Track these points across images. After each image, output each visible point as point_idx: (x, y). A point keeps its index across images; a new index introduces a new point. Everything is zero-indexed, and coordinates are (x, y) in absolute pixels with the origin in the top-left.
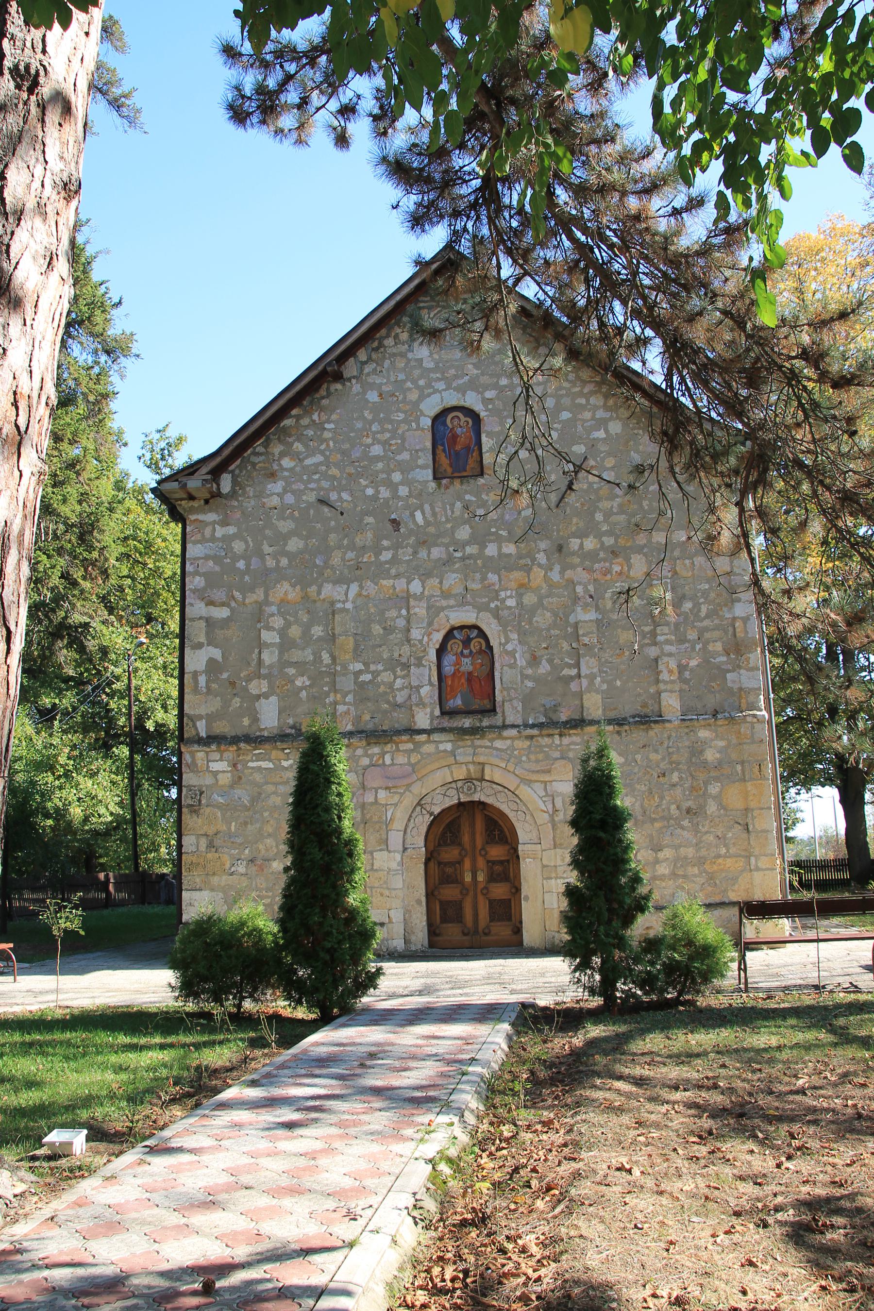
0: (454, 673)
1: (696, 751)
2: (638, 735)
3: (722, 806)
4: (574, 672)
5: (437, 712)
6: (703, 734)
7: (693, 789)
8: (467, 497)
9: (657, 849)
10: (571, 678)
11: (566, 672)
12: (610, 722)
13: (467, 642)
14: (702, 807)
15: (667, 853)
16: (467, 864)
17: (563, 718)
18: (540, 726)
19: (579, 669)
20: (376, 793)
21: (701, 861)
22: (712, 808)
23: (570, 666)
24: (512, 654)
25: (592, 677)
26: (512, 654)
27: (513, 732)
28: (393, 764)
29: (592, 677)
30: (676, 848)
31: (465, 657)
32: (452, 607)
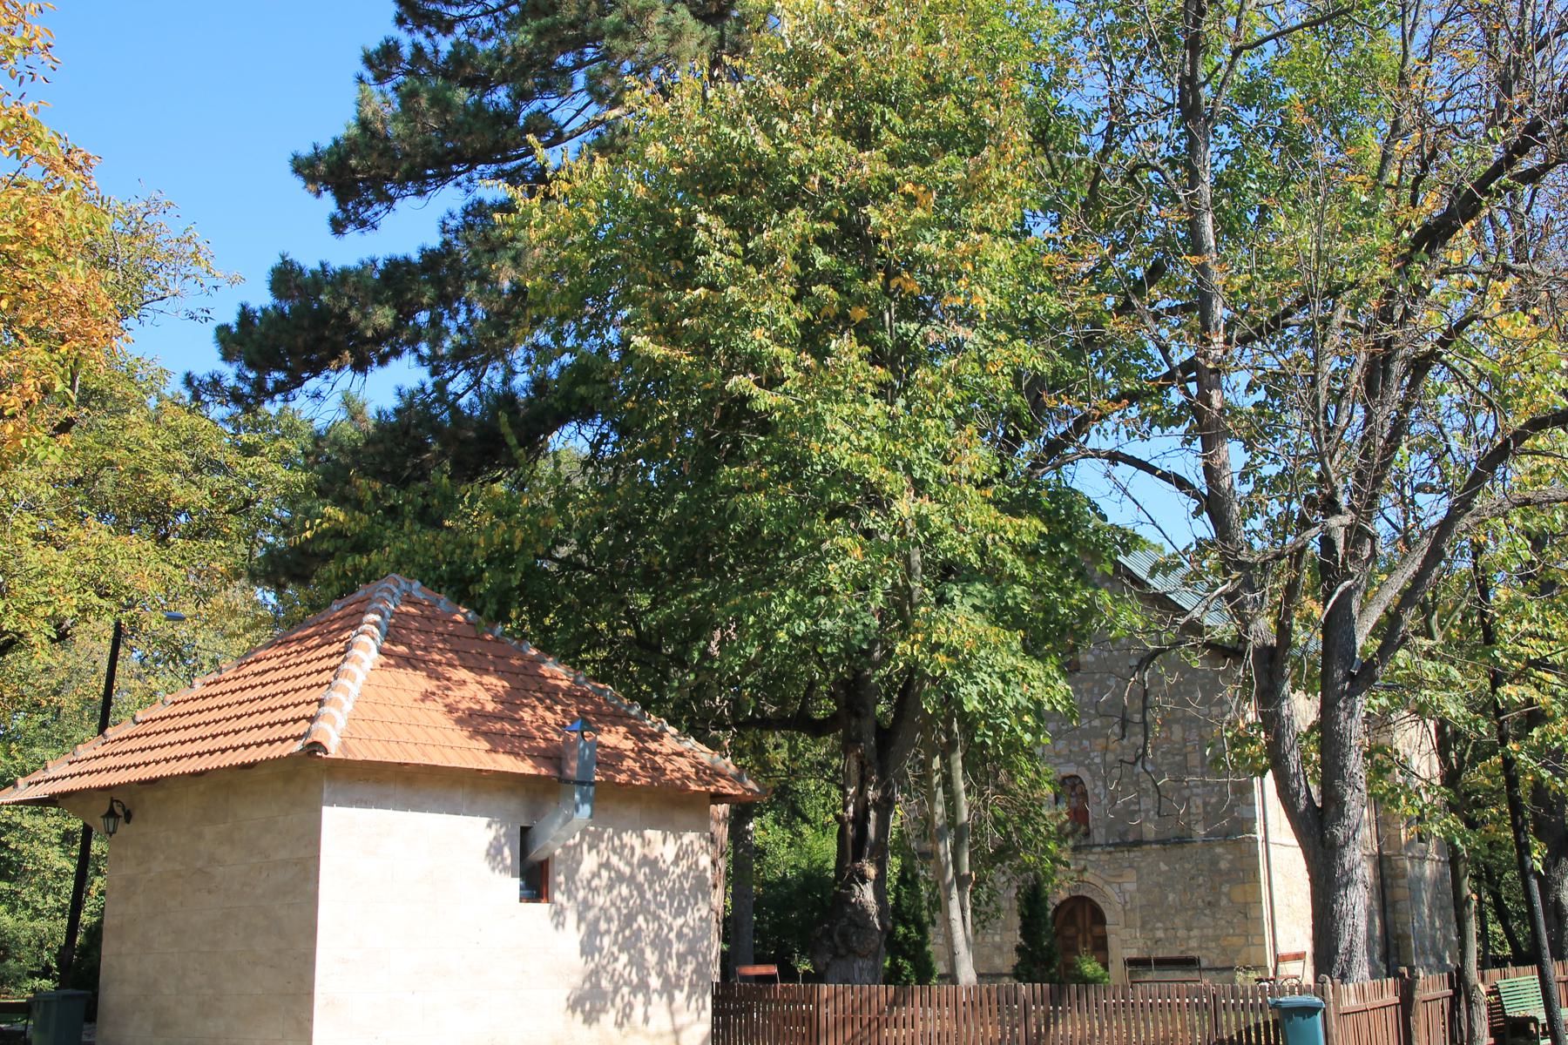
1: (1214, 862)
2: (1177, 852)
3: (1230, 900)
6: (1219, 850)
7: (1213, 888)
9: (1189, 929)
12: (1157, 842)
13: (1073, 787)
14: (1218, 901)
15: (1195, 932)
16: (1080, 938)
17: (1131, 838)
18: (1115, 845)
21: (1217, 938)
22: (1224, 902)
24: (1098, 796)
25: (1147, 811)
26: (1098, 796)
27: (1098, 849)
29: (1147, 811)
30: (1202, 928)
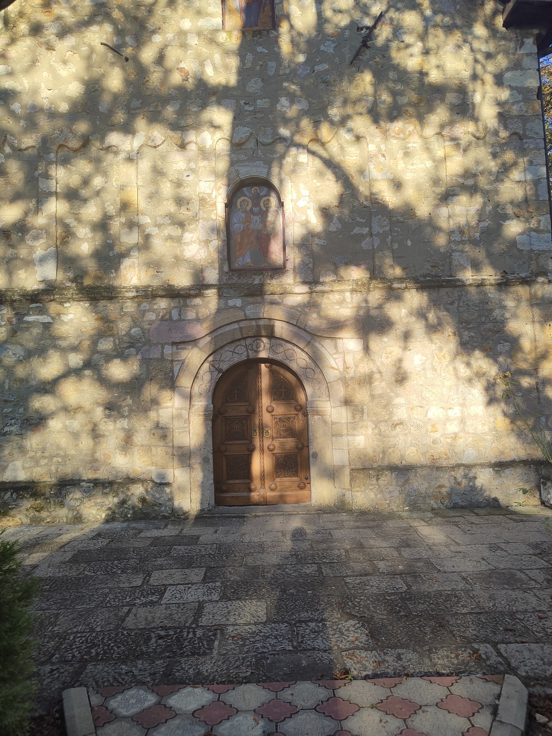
0: (244, 230)
4: (366, 230)
5: (226, 269)
8: (259, 49)
10: (363, 236)
11: (357, 230)
19: (371, 228)
20: (163, 348)
23: (361, 225)
28: (180, 320)
31: (254, 214)
32: (243, 161)
